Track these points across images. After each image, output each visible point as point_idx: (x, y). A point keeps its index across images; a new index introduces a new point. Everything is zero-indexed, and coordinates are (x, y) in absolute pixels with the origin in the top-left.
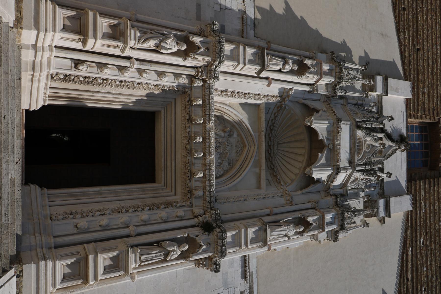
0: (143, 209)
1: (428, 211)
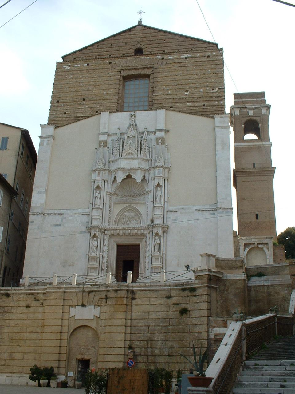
0: (146, 250)
1: (171, 87)
